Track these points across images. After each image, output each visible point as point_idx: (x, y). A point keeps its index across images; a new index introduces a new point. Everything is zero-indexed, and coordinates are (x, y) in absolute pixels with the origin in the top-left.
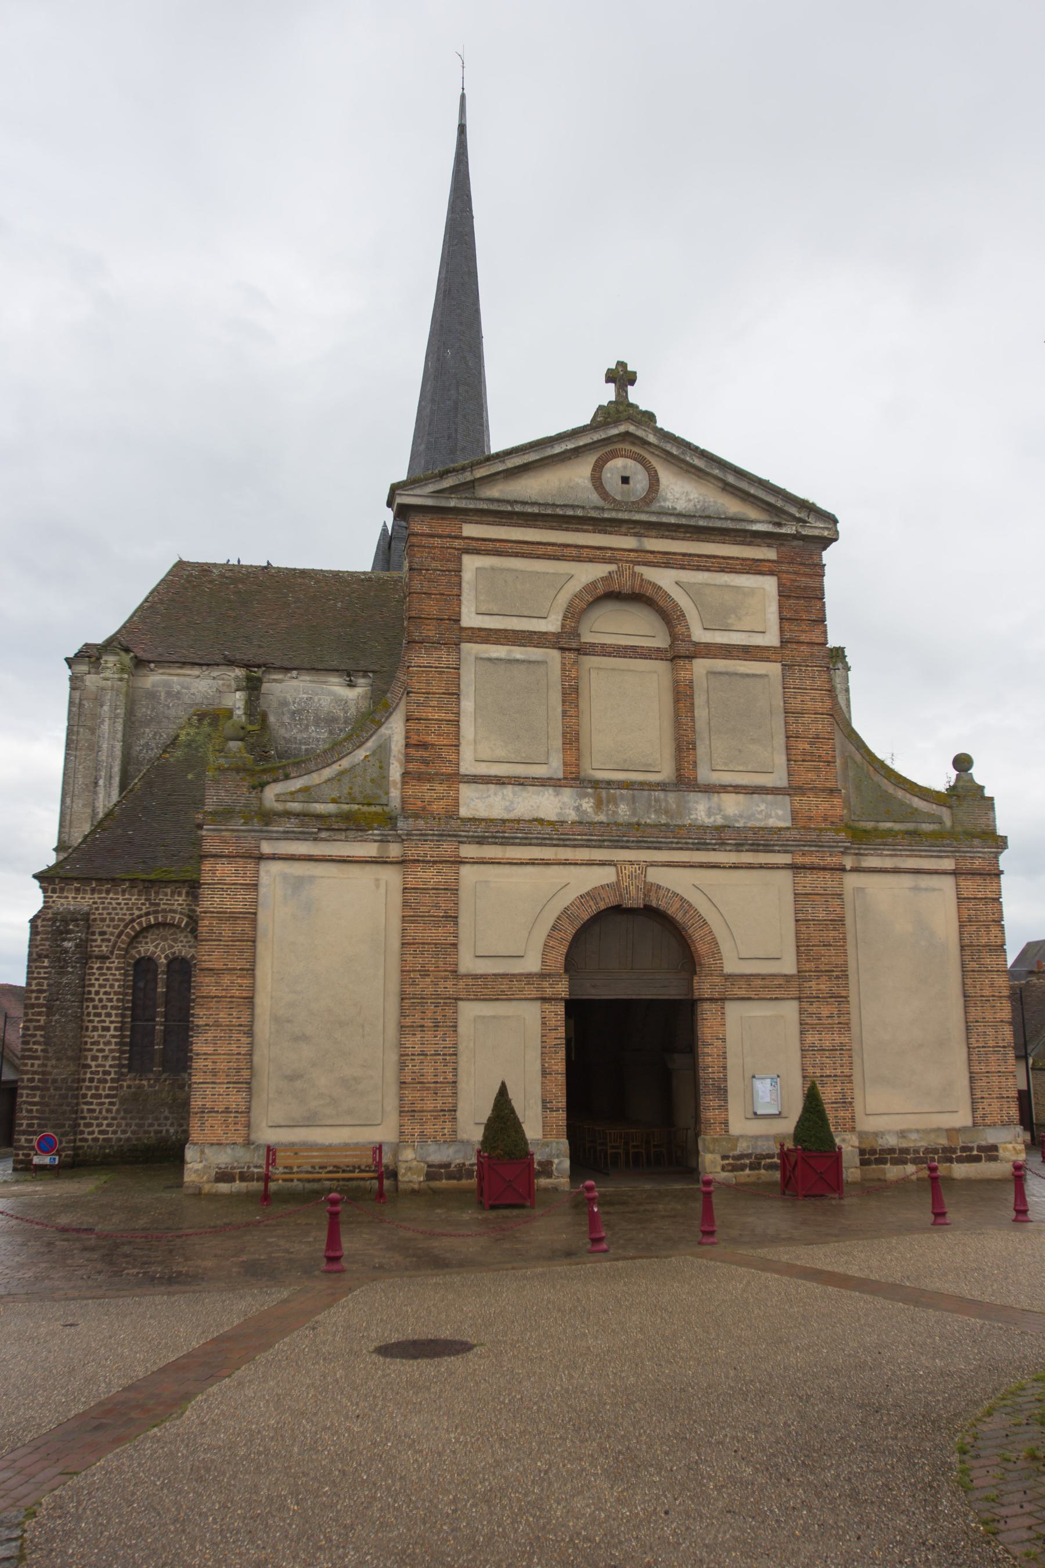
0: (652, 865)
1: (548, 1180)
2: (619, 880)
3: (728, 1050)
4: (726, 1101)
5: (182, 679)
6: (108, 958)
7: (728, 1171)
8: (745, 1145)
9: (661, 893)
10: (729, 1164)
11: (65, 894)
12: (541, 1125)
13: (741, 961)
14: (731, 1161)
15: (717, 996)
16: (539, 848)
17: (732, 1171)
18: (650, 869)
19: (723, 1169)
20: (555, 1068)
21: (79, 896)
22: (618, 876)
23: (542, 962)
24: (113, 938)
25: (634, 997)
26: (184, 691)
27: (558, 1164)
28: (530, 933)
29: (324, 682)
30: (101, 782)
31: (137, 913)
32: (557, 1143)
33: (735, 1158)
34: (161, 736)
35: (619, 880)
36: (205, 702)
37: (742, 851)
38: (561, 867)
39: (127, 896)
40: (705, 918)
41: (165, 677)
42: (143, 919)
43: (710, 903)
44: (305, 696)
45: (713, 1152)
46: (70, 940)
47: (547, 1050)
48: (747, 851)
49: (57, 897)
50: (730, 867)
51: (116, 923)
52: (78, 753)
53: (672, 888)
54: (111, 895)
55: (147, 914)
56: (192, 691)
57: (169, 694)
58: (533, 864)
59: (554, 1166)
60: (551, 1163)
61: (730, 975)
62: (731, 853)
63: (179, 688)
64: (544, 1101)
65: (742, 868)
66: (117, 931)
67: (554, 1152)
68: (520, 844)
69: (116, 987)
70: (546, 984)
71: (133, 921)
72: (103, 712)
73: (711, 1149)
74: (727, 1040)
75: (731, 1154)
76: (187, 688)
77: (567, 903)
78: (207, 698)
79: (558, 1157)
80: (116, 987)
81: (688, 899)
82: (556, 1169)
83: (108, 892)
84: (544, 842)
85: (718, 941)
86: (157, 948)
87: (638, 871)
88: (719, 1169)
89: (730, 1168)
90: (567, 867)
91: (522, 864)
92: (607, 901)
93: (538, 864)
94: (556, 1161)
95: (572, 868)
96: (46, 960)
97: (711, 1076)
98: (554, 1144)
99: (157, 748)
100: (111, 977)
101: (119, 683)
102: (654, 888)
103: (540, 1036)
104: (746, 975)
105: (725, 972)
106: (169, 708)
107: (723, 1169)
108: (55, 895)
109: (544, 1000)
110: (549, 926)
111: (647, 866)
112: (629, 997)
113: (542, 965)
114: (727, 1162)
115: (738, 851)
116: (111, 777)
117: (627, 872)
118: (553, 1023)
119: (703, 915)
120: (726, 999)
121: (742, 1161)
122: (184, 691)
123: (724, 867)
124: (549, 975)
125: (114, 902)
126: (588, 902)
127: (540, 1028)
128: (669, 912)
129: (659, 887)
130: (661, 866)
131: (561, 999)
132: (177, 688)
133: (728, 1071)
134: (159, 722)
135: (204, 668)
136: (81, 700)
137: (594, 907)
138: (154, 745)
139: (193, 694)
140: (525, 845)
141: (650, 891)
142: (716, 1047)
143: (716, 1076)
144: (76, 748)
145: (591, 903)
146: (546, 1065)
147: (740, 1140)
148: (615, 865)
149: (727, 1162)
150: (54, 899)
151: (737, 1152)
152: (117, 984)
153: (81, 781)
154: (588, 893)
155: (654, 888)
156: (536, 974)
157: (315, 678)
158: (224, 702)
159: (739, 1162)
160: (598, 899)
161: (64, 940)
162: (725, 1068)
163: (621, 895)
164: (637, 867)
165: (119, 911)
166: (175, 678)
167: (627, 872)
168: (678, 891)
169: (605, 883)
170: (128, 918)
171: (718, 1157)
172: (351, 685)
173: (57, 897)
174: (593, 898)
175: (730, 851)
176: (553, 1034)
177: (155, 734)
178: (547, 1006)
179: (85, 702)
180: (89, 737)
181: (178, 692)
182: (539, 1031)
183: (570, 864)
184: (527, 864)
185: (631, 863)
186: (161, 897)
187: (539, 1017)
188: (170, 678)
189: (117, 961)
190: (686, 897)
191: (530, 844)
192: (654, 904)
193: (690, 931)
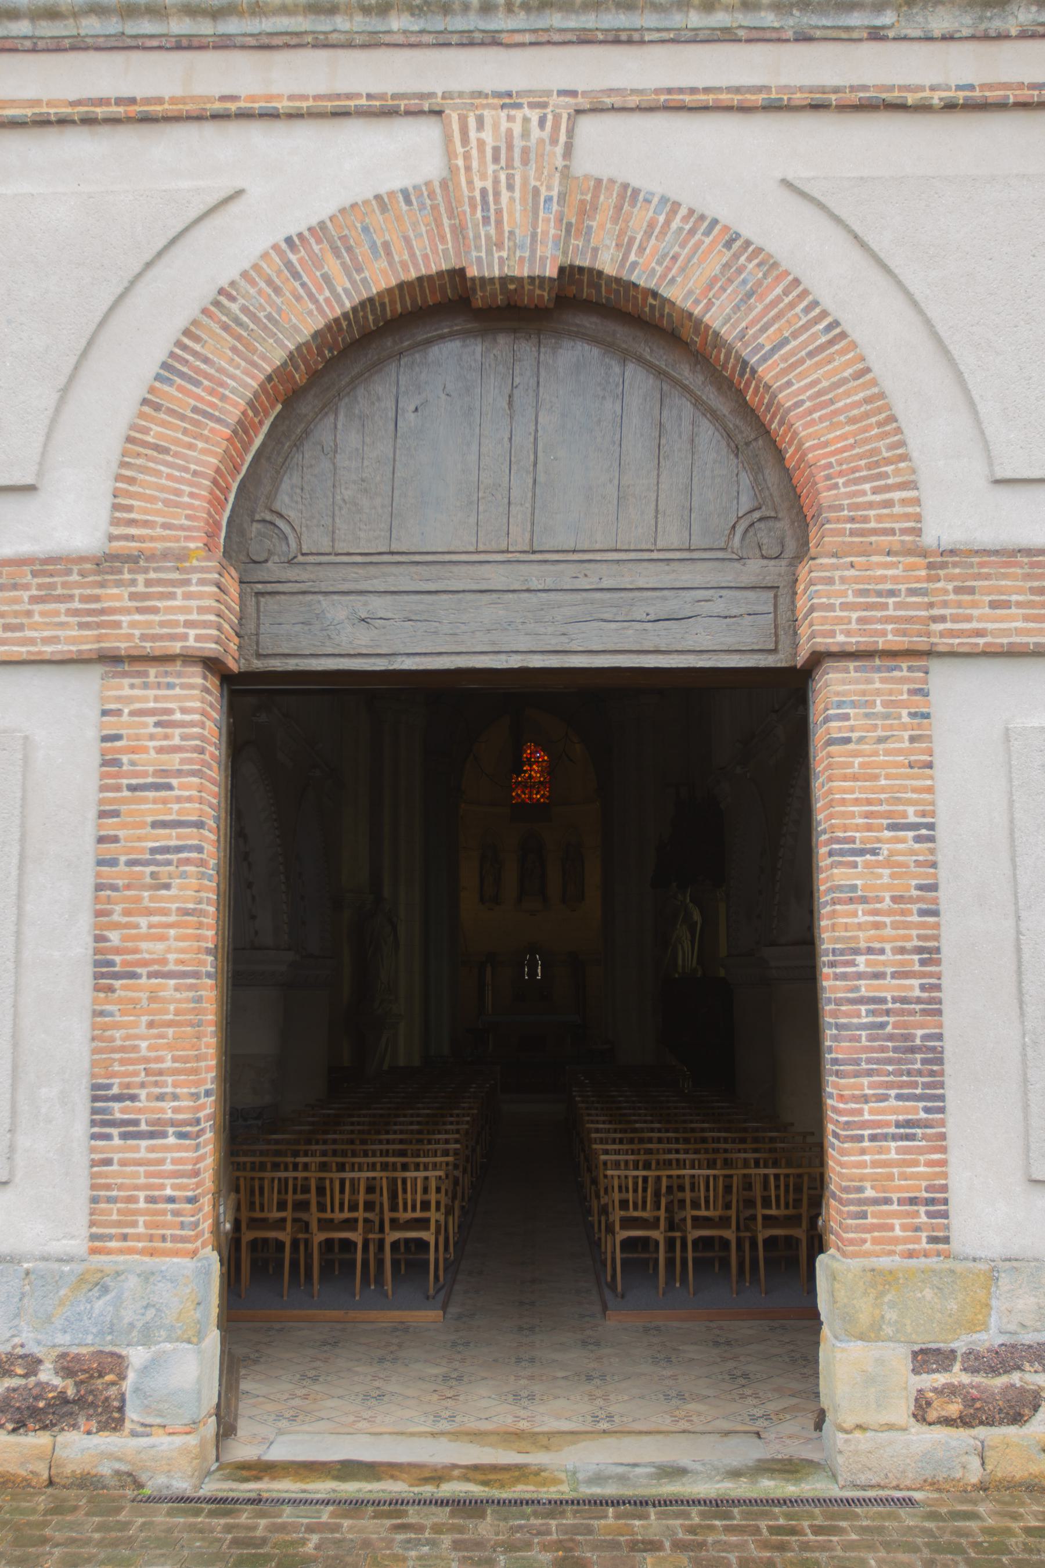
0: (597, 110)
1: (106, 1441)
2: (453, 170)
3: (943, 874)
4: (936, 1103)
7: (947, 1422)
8: (1025, 1303)
9: (639, 218)
10: (950, 1391)
12: (84, 1193)
13: (1004, 494)
14: (957, 1376)
15: (890, 639)
16: (119, 57)
17: (964, 1421)
18: (589, 127)
19: (921, 1412)
20: (150, 949)
22: (449, 153)
23: (116, 507)
25: (537, 662)
27: (145, 1370)
28: (65, 391)
32: (147, 1276)
33: (976, 1362)
35: (453, 170)
37: (1002, 37)
38: (209, 129)
40: (836, 313)
43: (856, 254)
45: (870, 1334)
47: (118, 875)
48: (1025, 35)
50: (950, 107)
53: (688, 200)
58: (89, 121)
59: (131, 1376)
60: (116, 1364)
61: (952, 552)
62: (953, 47)
64: (99, 1094)
65: (1001, 106)
67: (128, 1315)
68: (35, 47)
70: (116, 596)
73: (864, 1319)
74: (940, 833)
75: (960, 1345)
77: (228, 273)
79: (147, 1338)
81: (758, 241)
82: (136, 1390)
84: (134, 27)
85: (899, 409)
87: (536, 133)
88: (901, 1411)
89: (954, 1409)
90: (233, 128)
91: (43, 122)
92: (400, 254)
93: (113, 121)
94: (137, 1356)
95: (256, 134)
97: (865, 989)
98: (132, 1282)
102: (607, 201)
103: (92, 814)
104: (1028, 552)
105: (929, 539)
107: (921, 1412)
109: (110, 659)
110: (153, 368)
111: (578, 112)
112: (515, 662)
113: (115, 522)
114: (941, 1379)
115: (986, 37)
117: (487, 136)
118: (149, 761)
119: (827, 302)
120: (929, 654)
121: (1015, 1378)
123: (923, 108)
124: (132, 559)
126: (318, 263)
127: (93, 783)
128: (674, 293)
129: (629, 194)
130: (640, 109)
131: (187, 658)
133: (944, 968)
137: (342, 283)
140: (56, 47)
141: (586, 211)
142: (888, 864)
143: (889, 989)
145: (333, 266)
146: (114, 937)
147: (1004, 1280)
148: (437, 113)
149: (941, 1379)
151: (988, 1339)
154: (319, 230)
155: (607, 201)
156: (82, 559)
159: (999, 1382)
160: (363, 251)
162: (930, 955)
163: (459, 231)
164: (534, 115)
167: (487, 136)
168: (714, 208)
169: (396, 185)
171: (899, 1358)
174: (341, 247)
175: (948, 38)
176: (149, 807)
178: (124, 687)
182: (92, 794)
183: (244, 115)
184: (63, 122)
185: (508, 100)
187: (92, 733)
190: (746, 233)
191: (78, 45)
192: (608, 263)
193: (767, 372)
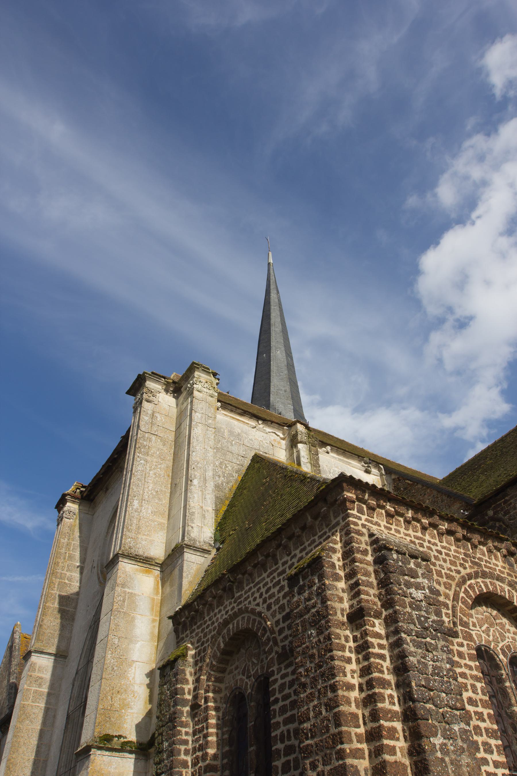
5: (241, 425)
6: (455, 635)
11: (375, 519)
21: (393, 527)
24: (450, 603)
26: (244, 435)
29: (349, 464)
30: (195, 482)
31: (463, 572)
34: (226, 467)
36: (261, 449)
39: (445, 544)
41: (228, 419)
42: (473, 581)
44: (336, 469)
46: (418, 587)
49: (366, 520)
51: (445, 580)
52: (149, 458)
54: (427, 537)
55: (476, 575)
56: (250, 437)
57: (231, 432)
63: (240, 431)
66: (451, 593)
69: (479, 691)
71: (463, 581)
72: (196, 417)
76: (245, 433)
78: (263, 447)
80: (479, 691)
83: (424, 529)
86: (489, 636)
96: (377, 622)
99: (224, 476)
100: (467, 671)
101: (210, 398)
106: (232, 445)
108: (364, 517)
116: (205, 480)
122: (244, 435)
125: (434, 548)
132: (237, 431)
134: (225, 454)
135: (260, 422)
136: (154, 412)
138: (220, 473)
139: (251, 440)
144: (148, 453)
150: (363, 522)
152: (479, 685)
153: (151, 486)
157: (341, 458)
158: (276, 454)
161: (408, 585)
165: (441, 563)
166: (236, 423)
170: (457, 577)
172: (368, 472)
173: (366, 520)
177: (221, 463)
179: (157, 415)
180: (161, 447)
181: (239, 434)
186: (478, 555)
188: (232, 421)
189: (465, 643)
